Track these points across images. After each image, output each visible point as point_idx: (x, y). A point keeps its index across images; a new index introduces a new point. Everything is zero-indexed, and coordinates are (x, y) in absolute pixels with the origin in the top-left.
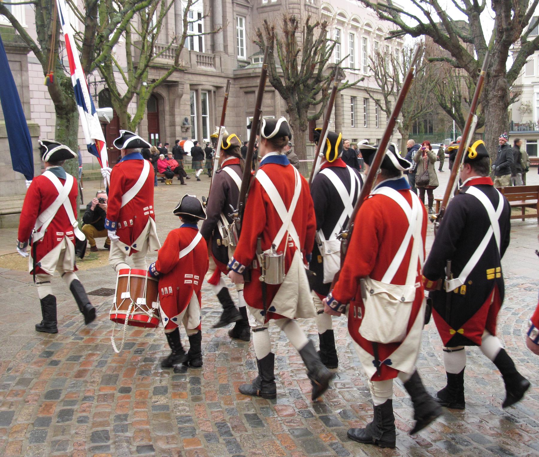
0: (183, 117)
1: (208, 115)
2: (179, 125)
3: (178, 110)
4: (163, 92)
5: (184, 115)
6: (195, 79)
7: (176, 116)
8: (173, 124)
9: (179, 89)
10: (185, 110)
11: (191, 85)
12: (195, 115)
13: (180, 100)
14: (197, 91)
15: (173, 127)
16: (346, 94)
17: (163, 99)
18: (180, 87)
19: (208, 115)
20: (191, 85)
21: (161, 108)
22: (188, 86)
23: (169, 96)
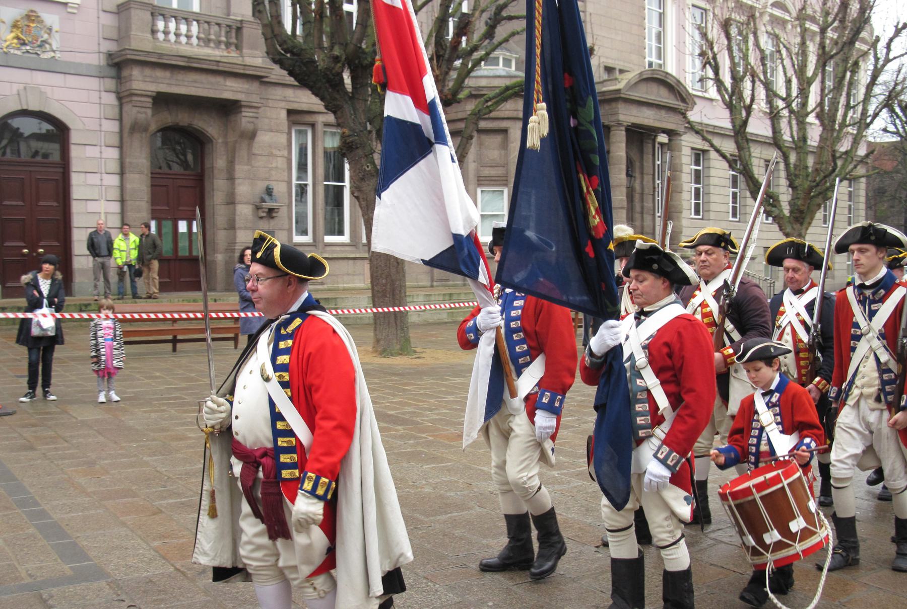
0: (261, 186)
1: (347, 183)
2: (247, 203)
3: (246, 167)
4: (210, 126)
5: (267, 179)
6: (304, 100)
7: (237, 181)
8: (231, 201)
9: (244, 120)
10: (271, 169)
11: (290, 112)
12: (310, 181)
13: (250, 146)
14: (313, 126)
15: (231, 206)
16: (689, 141)
17: (212, 141)
18: (246, 113)
19: (347, 183)
20: (290, 112)
21: (207, 164)
22: (283, 114)
23: (225, 136)
